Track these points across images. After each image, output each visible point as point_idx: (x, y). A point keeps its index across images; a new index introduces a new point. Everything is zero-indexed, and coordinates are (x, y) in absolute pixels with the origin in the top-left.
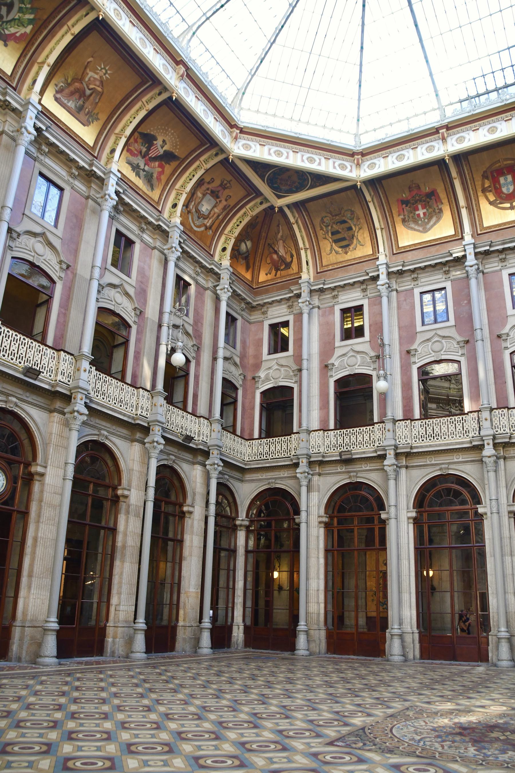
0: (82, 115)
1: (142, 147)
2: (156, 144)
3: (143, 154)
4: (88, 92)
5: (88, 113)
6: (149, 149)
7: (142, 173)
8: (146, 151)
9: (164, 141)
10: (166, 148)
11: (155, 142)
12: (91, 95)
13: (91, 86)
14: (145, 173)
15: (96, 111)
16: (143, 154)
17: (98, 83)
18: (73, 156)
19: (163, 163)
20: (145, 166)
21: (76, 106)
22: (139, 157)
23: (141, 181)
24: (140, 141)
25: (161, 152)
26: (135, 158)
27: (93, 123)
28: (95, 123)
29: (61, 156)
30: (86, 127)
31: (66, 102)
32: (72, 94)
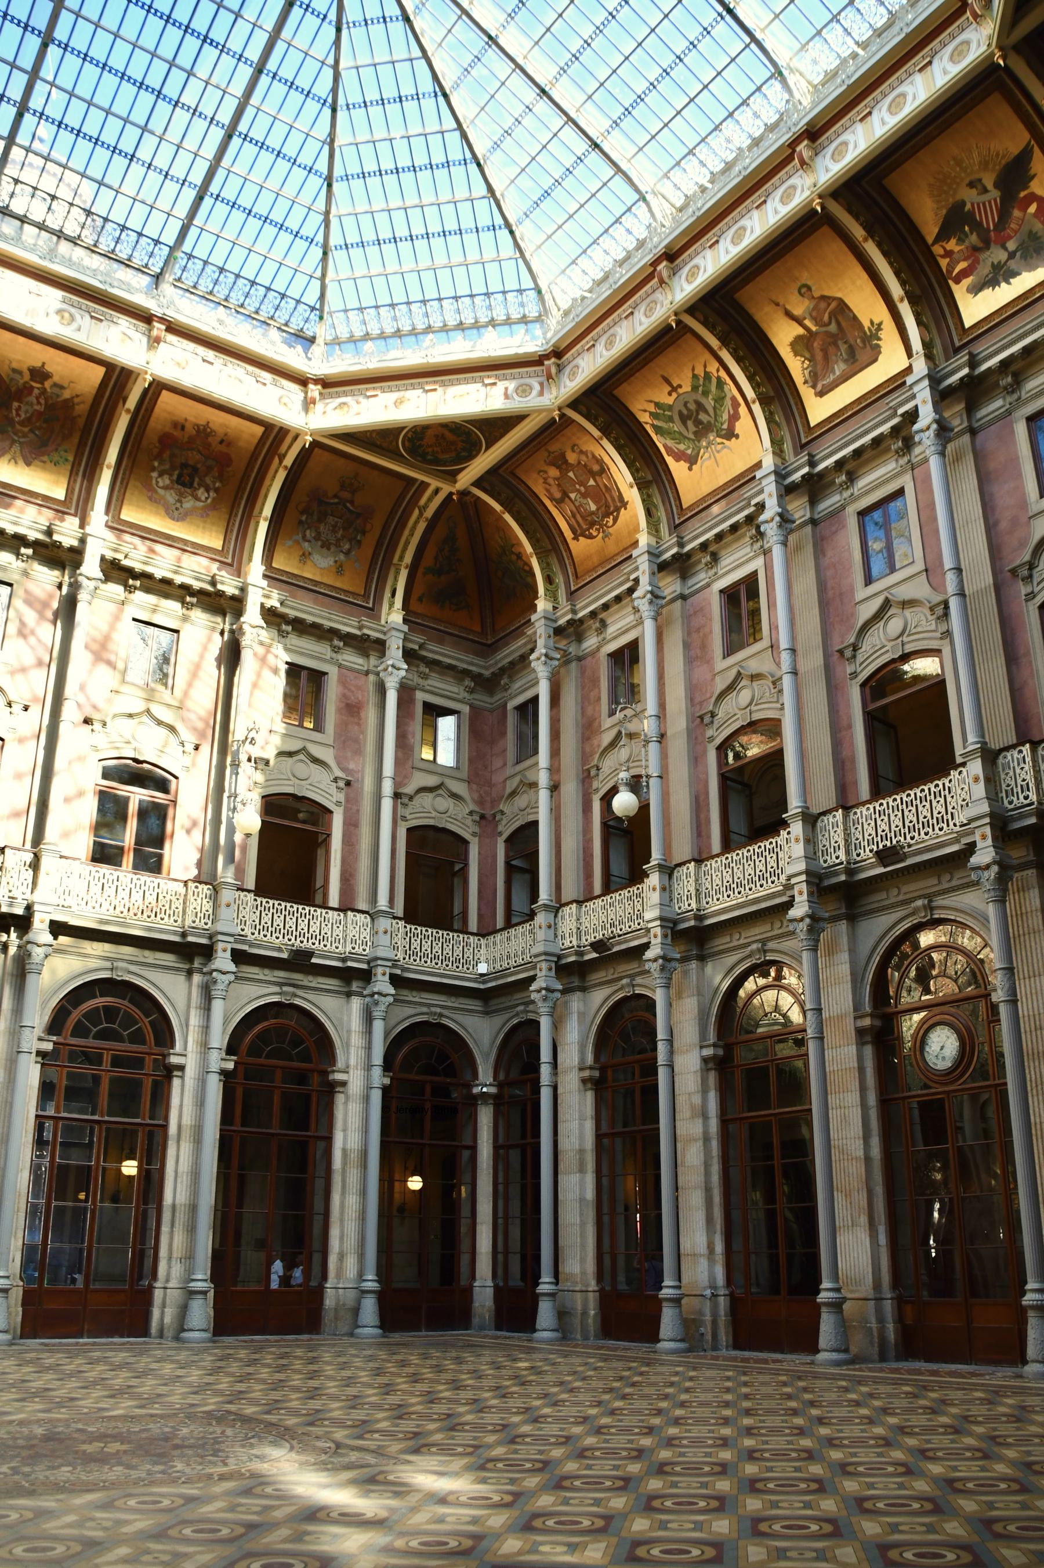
0: (862, 356)
1: (967, 243)
2: (973, 205)
3: (980, 245)
4: (833, 328)
5: (864, 342)
6: (977, 226)
7: (1013, 264)
8: (978, 235)
9: (971, 185)
10: (989, 181)
11: (968, 207)
12: (838, 324)
13: (826, 318)
14: (1018, 254)
15: (866, 324)
16: (980, 245)
17: (823, 305)
18: (867, 439)
19: (1022, 194)
20: (1006, 249)
21: (845, 361)
22: (982, 256)
23: (1025, 275)
24: (952, 245)
25: (995, 194)
26: (980, 268)
27: (879, 339)
28: (882, 334)
29: (865, 456)
30: (880, 358)
31: (832, 377)
32: (826, 358)
